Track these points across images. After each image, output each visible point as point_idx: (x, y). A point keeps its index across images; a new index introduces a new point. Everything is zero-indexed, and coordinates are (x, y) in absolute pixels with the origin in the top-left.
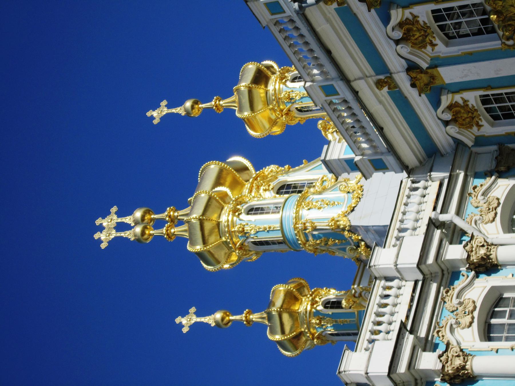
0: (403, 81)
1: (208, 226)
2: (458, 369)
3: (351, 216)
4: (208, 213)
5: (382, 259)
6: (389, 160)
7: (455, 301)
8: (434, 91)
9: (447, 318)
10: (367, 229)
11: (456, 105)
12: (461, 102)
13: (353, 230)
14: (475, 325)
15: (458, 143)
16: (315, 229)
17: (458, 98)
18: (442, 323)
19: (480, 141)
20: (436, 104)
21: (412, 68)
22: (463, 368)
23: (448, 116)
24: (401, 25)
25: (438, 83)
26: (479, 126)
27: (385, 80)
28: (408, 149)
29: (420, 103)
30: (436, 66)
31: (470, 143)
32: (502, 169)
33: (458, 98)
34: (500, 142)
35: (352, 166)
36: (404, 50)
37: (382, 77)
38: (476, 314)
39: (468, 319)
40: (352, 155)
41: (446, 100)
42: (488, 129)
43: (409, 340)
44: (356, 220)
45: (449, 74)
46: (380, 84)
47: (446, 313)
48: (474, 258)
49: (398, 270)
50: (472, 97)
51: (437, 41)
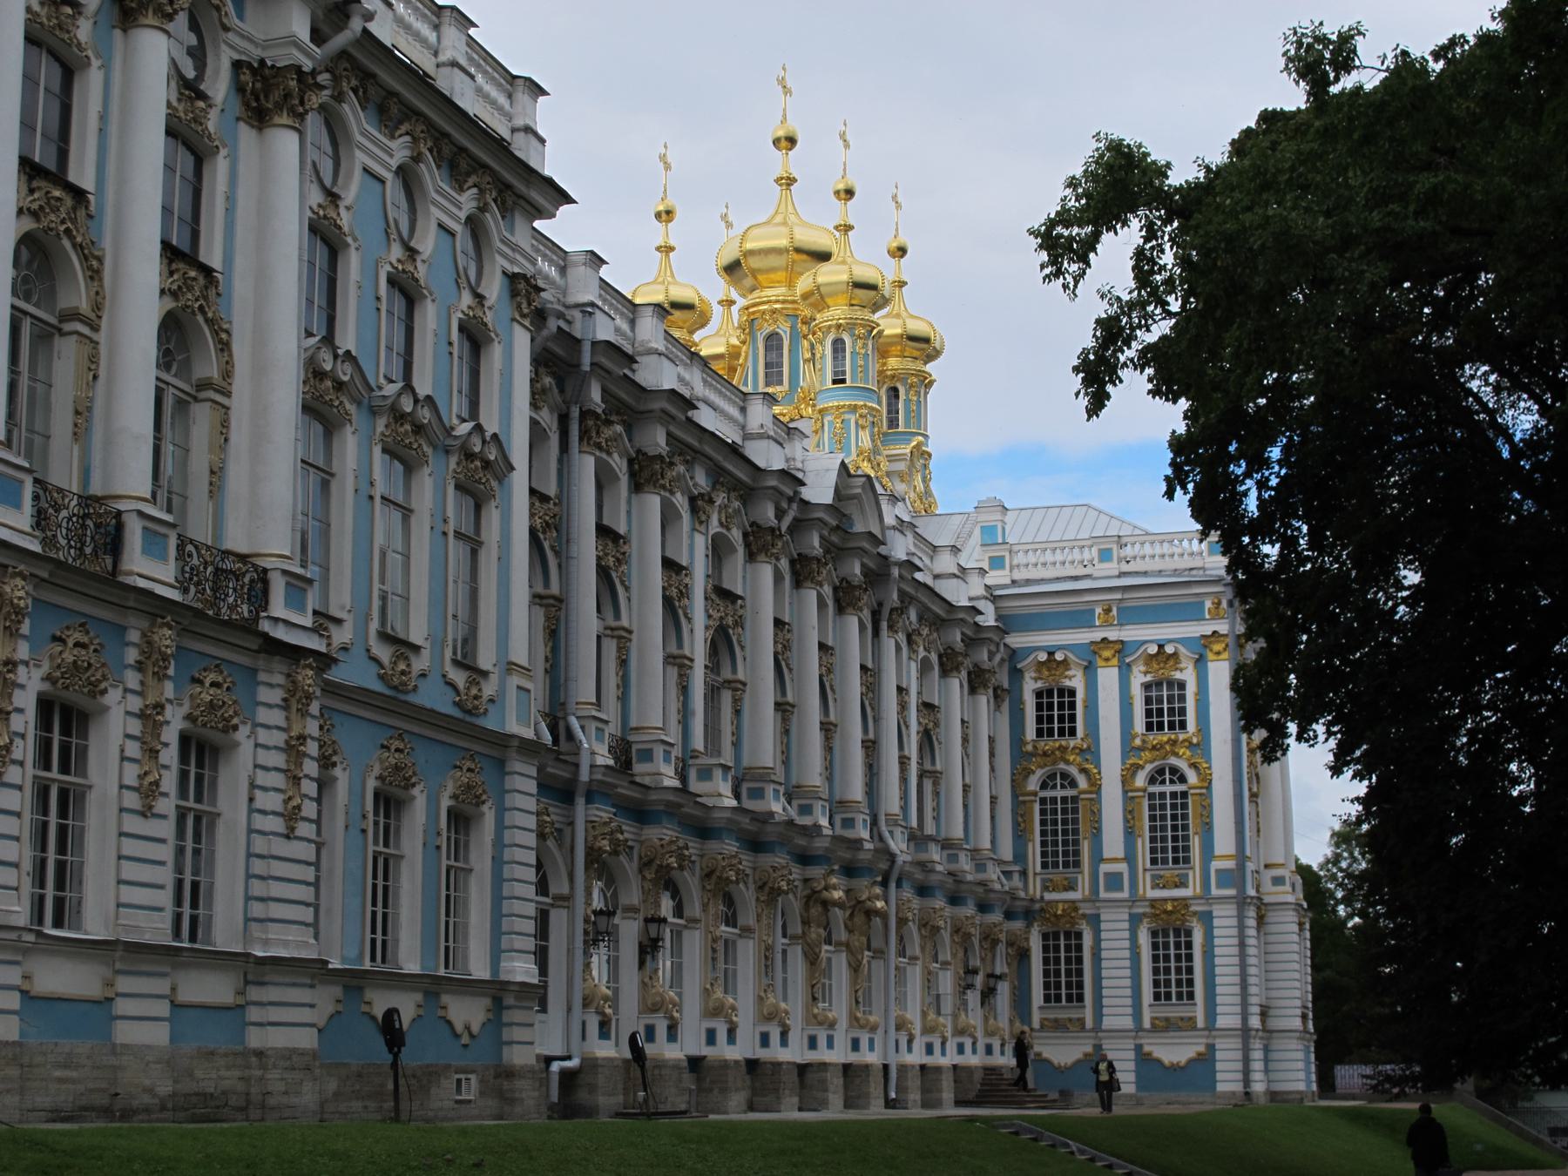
23: (1059, 656)
26: (1036, 679)
42: (1030, 686)
45: (1108, 677)
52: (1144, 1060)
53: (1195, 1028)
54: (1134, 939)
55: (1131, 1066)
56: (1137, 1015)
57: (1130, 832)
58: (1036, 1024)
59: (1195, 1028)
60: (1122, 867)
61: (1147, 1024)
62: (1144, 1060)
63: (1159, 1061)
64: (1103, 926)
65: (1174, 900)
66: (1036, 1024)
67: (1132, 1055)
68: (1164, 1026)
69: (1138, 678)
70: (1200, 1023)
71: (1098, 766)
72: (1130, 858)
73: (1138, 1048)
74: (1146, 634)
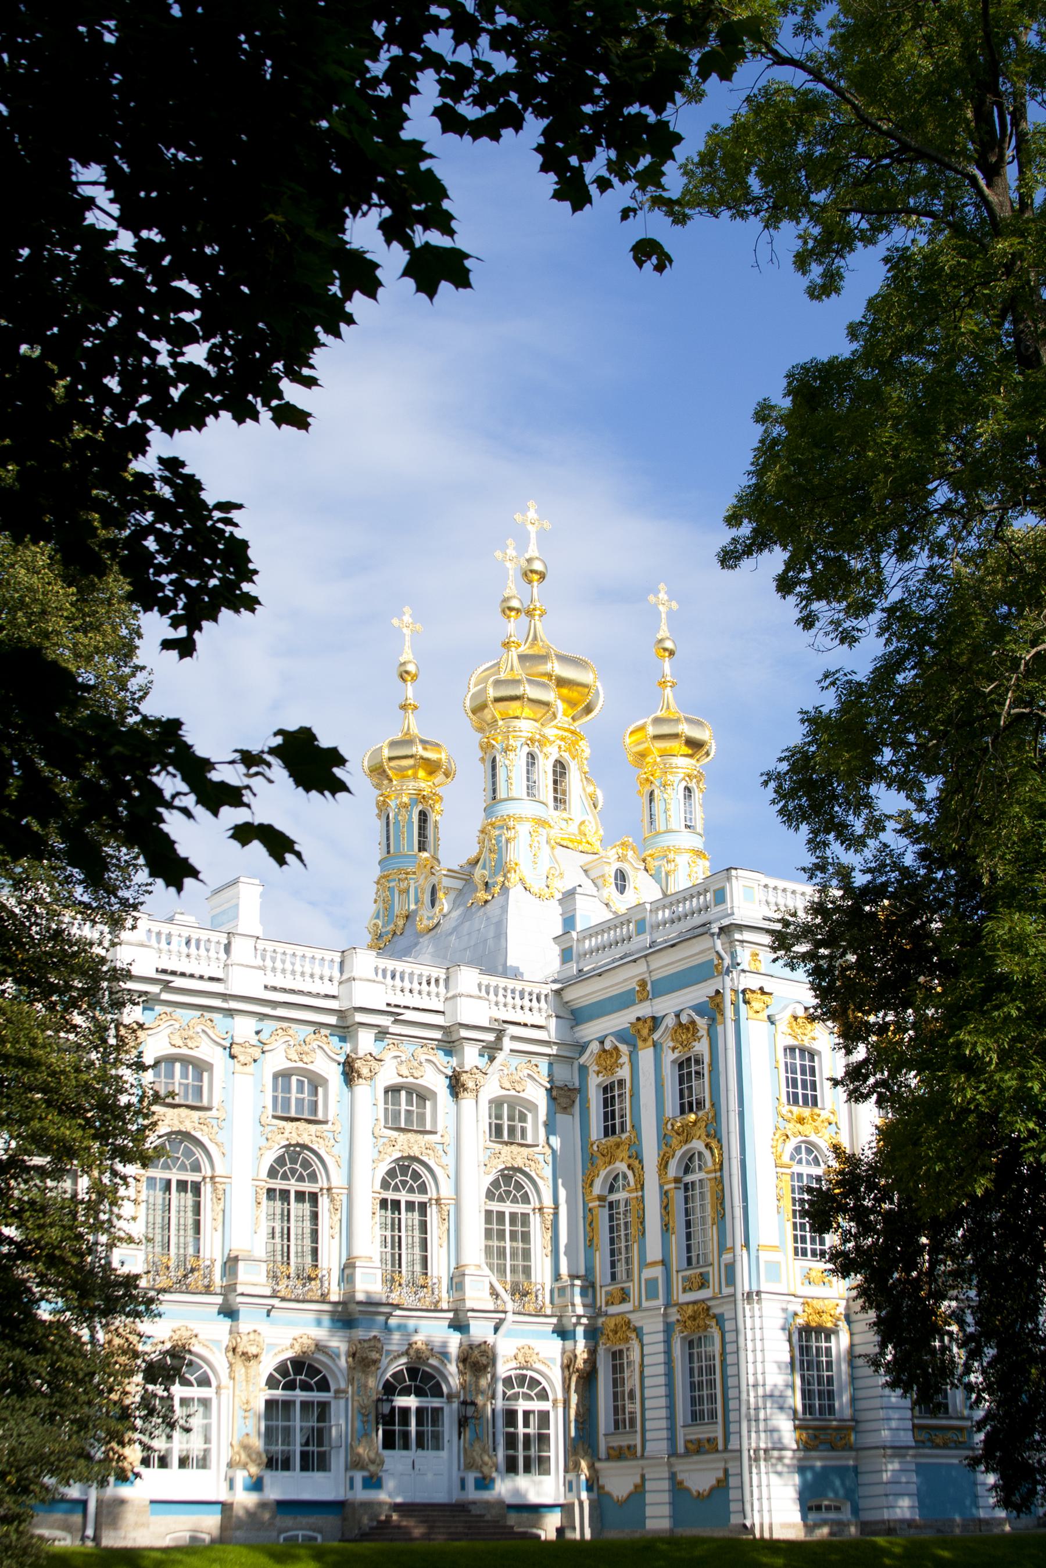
0: (644, 1010)
1: (514, 707)
2: (358, 1072)
3: (520, 887)
4: (531, 704)
5: (468, 978)
6: (573, 968)
7: (423, 1058)
8: (631, 1037)
9: (408, 1049)
10: (504, 909)
11: (619, 1056)
12: (621, 1061)
13: (505, 889)
14: (400, 1080)
15: (582, 1048)
16: (508, 841)
17: (624, 1059)
18: (402, 1047)
19: (583, 1069)
20: (622, 1036)
21: (655, 1022)
22: (359, 1076)
23: (608, 1046)
24: (693, 1022)
25: (640, 1044)
26: (598, 1073)
27: (645, 991)
28: (581, 995)
29: (622, 1020)
30: (654, 1046)
31: (582, 1060)
32: (554, 1093)
33: (624, 1059)
34: (581, 1090)
35: (569, 922)
36: (670, 1021)
37: (649, 988)
38: (411, 1080)
39: (405, 1073)
40: (579, 928)
41: (624, 1048)
42: (594, 1082)
43: (385, 1021)
44: (516, 893)
45: (646, 1056)
46: (643, 984)
47: (412, 1048)
48: (464, 1077)
49: (454, 997)
50: (624, 1073)
51: (676, 1054)
52: (677, 1488)
53: (717, 1451)
54: (668, 1352)
55: (666, 1497)
56: (672, 1439)
57: (666, 1228)
58: (602, 1454)
59: (717, 1451)
60: (657, 1272)
61: (681, 1449)
62: (677, 1488)
63: (688, 1490)
64: (646, 1339)
65: (695, 1303)
66: (602, 1454)
67: (665, 1485)
68: (698, 1448)
69: (669, 1057)
70: (720, 1447)
71: (641, 1162)
72: (665, 1262)
73: (673, 1476)
74: (665, 1006)
